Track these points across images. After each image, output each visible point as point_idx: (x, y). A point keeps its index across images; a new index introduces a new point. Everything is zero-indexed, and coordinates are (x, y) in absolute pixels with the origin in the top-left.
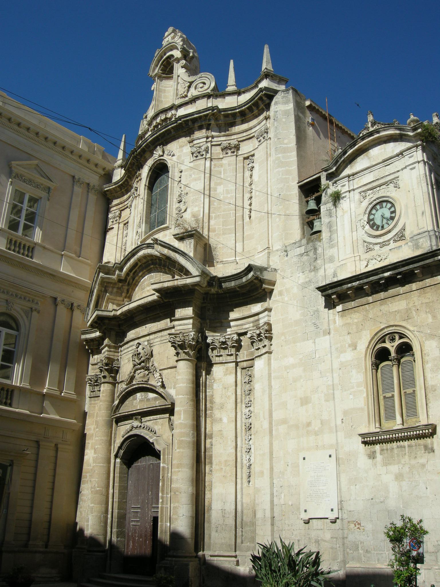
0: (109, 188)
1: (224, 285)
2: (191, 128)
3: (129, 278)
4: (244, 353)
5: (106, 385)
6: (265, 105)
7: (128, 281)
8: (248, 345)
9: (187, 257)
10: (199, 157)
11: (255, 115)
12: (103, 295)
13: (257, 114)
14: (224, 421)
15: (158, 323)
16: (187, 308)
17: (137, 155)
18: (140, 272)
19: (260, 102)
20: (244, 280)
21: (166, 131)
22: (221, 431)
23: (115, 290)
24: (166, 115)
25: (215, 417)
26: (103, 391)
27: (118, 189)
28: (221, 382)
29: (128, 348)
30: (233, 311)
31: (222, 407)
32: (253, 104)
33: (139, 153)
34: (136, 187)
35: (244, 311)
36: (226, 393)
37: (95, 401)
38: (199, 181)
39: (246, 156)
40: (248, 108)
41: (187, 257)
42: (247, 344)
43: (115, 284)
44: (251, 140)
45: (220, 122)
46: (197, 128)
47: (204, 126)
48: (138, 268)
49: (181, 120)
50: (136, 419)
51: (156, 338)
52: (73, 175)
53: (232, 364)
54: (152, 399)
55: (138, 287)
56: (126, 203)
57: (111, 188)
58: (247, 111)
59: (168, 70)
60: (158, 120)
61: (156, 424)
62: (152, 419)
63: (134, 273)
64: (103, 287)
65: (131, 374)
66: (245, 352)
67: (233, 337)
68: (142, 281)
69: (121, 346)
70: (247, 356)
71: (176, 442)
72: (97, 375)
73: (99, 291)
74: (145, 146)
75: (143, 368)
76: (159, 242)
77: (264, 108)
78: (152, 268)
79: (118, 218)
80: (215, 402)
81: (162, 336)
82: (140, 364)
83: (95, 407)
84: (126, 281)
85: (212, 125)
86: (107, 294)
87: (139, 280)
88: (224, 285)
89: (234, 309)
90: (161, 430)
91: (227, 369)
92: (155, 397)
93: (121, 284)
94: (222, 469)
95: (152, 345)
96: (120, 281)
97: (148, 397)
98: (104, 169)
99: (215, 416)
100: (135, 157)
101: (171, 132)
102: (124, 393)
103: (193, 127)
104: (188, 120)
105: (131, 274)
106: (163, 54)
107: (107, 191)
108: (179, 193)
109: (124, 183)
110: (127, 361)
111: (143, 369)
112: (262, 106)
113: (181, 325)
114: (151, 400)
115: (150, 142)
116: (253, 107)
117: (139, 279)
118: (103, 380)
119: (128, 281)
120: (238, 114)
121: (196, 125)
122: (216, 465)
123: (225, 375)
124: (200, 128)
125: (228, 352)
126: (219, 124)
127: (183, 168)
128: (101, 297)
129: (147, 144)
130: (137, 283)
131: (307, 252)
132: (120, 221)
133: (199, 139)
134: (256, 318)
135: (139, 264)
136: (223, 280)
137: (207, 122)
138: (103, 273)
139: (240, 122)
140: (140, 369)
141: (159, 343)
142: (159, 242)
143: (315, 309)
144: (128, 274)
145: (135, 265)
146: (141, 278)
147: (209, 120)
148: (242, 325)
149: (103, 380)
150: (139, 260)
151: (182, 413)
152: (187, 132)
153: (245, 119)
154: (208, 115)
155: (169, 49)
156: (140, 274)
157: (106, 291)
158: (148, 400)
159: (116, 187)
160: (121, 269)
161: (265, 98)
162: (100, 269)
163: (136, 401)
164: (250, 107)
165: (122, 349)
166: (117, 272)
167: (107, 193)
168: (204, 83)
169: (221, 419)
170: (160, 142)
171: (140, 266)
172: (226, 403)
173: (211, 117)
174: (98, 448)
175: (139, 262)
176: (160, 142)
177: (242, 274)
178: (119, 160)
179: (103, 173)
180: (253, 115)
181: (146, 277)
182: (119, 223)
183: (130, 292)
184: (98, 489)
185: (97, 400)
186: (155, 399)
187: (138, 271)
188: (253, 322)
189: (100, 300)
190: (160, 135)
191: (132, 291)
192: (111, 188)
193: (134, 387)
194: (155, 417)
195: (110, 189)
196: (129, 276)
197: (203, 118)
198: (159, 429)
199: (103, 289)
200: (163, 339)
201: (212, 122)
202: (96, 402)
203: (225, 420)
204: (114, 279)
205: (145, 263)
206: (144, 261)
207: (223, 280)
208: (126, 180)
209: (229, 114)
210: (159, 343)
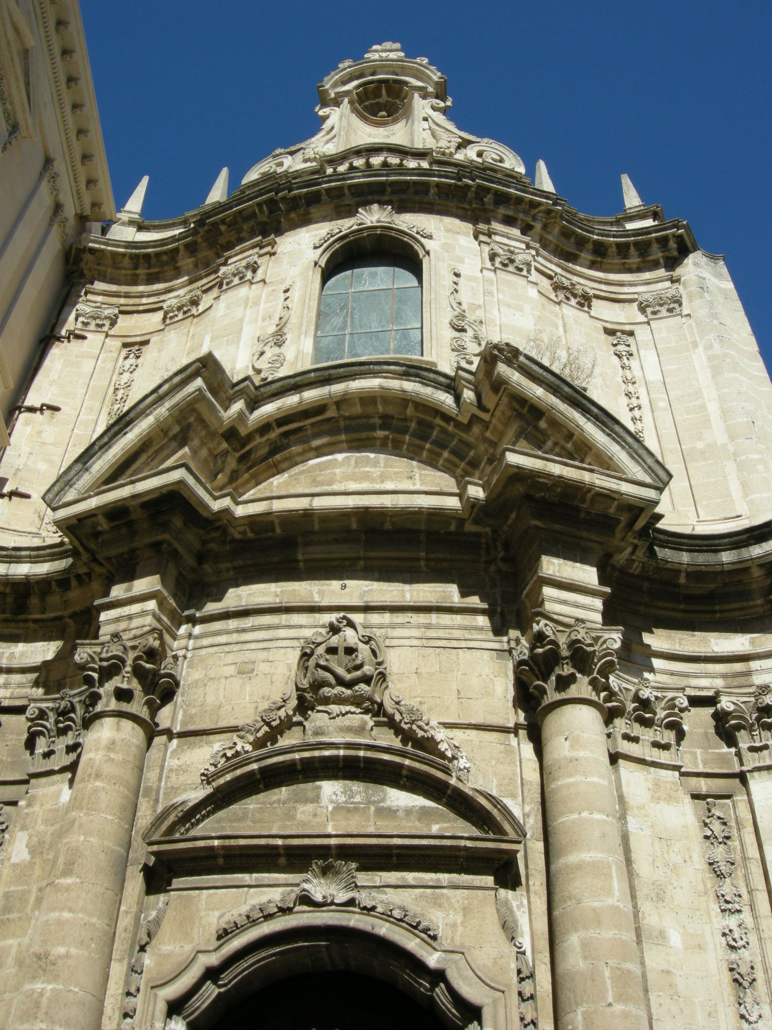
0: (103, 247)
1: (662, 553)
2: (485, 210)
3: (258, 440)
4: (695, 753)
5: (127, 725)
6: (667, 259)
7: (247, 448)
8: (706, 734)
9: (617, 428)
10: (511, 268)
11: (627, 266)
12: (161, 449)
13: (634, 266)
14: (672, 944)
15: (407, 587)
16: (578, 565)
17: (284, 199)
19: (655, 247)
20: (727, 557)
21: (415, 183)
23: (204, 453)
24: (402, 160)
25: (645, 922)
26: (113, 742)
27: (127, 262)
28: (647, 816)
29: (244, 630)
30: (652, 632)
31: (659, 897)
32: (636, 244)
33: (295, 198)
34: (255, 263)
35: (684, 642)
36: (666, 855)
38: (521, 313)
39: (609, 326)
40: (618, 245)
41: (617, 428)
42: (700, 730)
43: (212, 435)
44: (617, 305)
45: (550, 237)
46: (500, 216)
47: (519, 222)
48: (313, 424)
49: (473, 180)
50: (325, 872)
51: (402, 626)
52: (52, 154)
53: (670, 772)
55: (286, 475)
56: (162, 298)
57: (109, 248)
58: (614, 249)
59: (367, 103)
60: (376, 161)
61: (437, 903)
62: (413, 883)
63: (286, 435)
64: (178, 422)
65: (282, 713)
67: (673, 699)
68: (312, 462)
69: (193, 620)
71: (607, 973)
73: (161, 429)
74: (328, 190)
75: (357, 701)
76: (522, 358)
77: (662, 261)
78: (375, 439)
79: (107, 323)
80: (638, 875)
81: (428, 627)
82: (349, 685)
84: (243, 447)
85: (534, 230)
86: (186, 449)
87: (298, 459)
88: (662, 553)
89: (654, 630)
90: (460, 929)
93: (225, 445)
96: (231, 434)
97: (383, 800)
98: (95, 205)
99: (644, 918)
100: (271, 203)
101: (427, 192)
102: (255, 766)
103: (492, 211)
104: (488, 190)
105: (274, 435)
106: (368, 72)
107: (92, 251)
108: (456, 313)
109: (158, 255)
110: (232, 670)
111: (358, 705)
112: (656, 253)
113: (564, 602)
114: (401, 814)
115: (350, 187)
116: (632, 249)
117: (304, 452)
118: (113, 705)
119: (247, 448)
120: (590, 246)
121: (502, 211)
123: (656, 799)
124: (509, 221)
126: (546, 239)
127: (460, 269)
128: (151, 451)
129: (340, 188)
130: (284, 465)
132: (111, 332)
133: (509, 238)
134: (738, 667)
135: (331, 413)
136: (661, 536)
137: (529, 220)
138: (205, 381)
139: (588, 263)
142: (522, 358)
144: (265, 428)
145: (319, 409)
146: (312, 454)
147: (534, 218)
149: (113, 705)
150: (342, 401)
151: (614, 874)
152: (469, 213)
153: (601, 262)
154: (540, 204)
155: (387, 69)
156: (316, 443)
157: (182, 440)
158: (390, 813)
159: (124, 255)
160: (253, 405)
161: (672, 245)
162: (204, 366)
163: (310, 807)
164: (627, 245)
165: (198, 630)
166: (238, 406)
167: (87, 257)
169: (662, 935)
170: (386, 198)
171: (329, 420)
172: (672, 888)
173: (541, 214)
174: (67, 955)
175: (334, 407)
176: (386, 198)
177: (726, 540)
178: (125, 211)
179: (79, 212)
180: (624, 264)
181: (340, 457)
182: (107, 336)
183: (240, 481)
186: (423, 813)
187: (309, 432)
189: (143, 458)
190: (393, 183)
191: (248, 481)
192: (109, 248)
193: (327, 753)
194: (429, 877)
195: (102, 251)
196: (262, 435)
197: (523, 206)
198: (454, 926)
199: (176, 429)
200: (432, 633)
201: (538, 226)
203: (675, 939)
204: (220, 419)
205: (350, 418)
206: (358, 410)
207: (661, 536)
208: (176, 251)
209: (574, 233)
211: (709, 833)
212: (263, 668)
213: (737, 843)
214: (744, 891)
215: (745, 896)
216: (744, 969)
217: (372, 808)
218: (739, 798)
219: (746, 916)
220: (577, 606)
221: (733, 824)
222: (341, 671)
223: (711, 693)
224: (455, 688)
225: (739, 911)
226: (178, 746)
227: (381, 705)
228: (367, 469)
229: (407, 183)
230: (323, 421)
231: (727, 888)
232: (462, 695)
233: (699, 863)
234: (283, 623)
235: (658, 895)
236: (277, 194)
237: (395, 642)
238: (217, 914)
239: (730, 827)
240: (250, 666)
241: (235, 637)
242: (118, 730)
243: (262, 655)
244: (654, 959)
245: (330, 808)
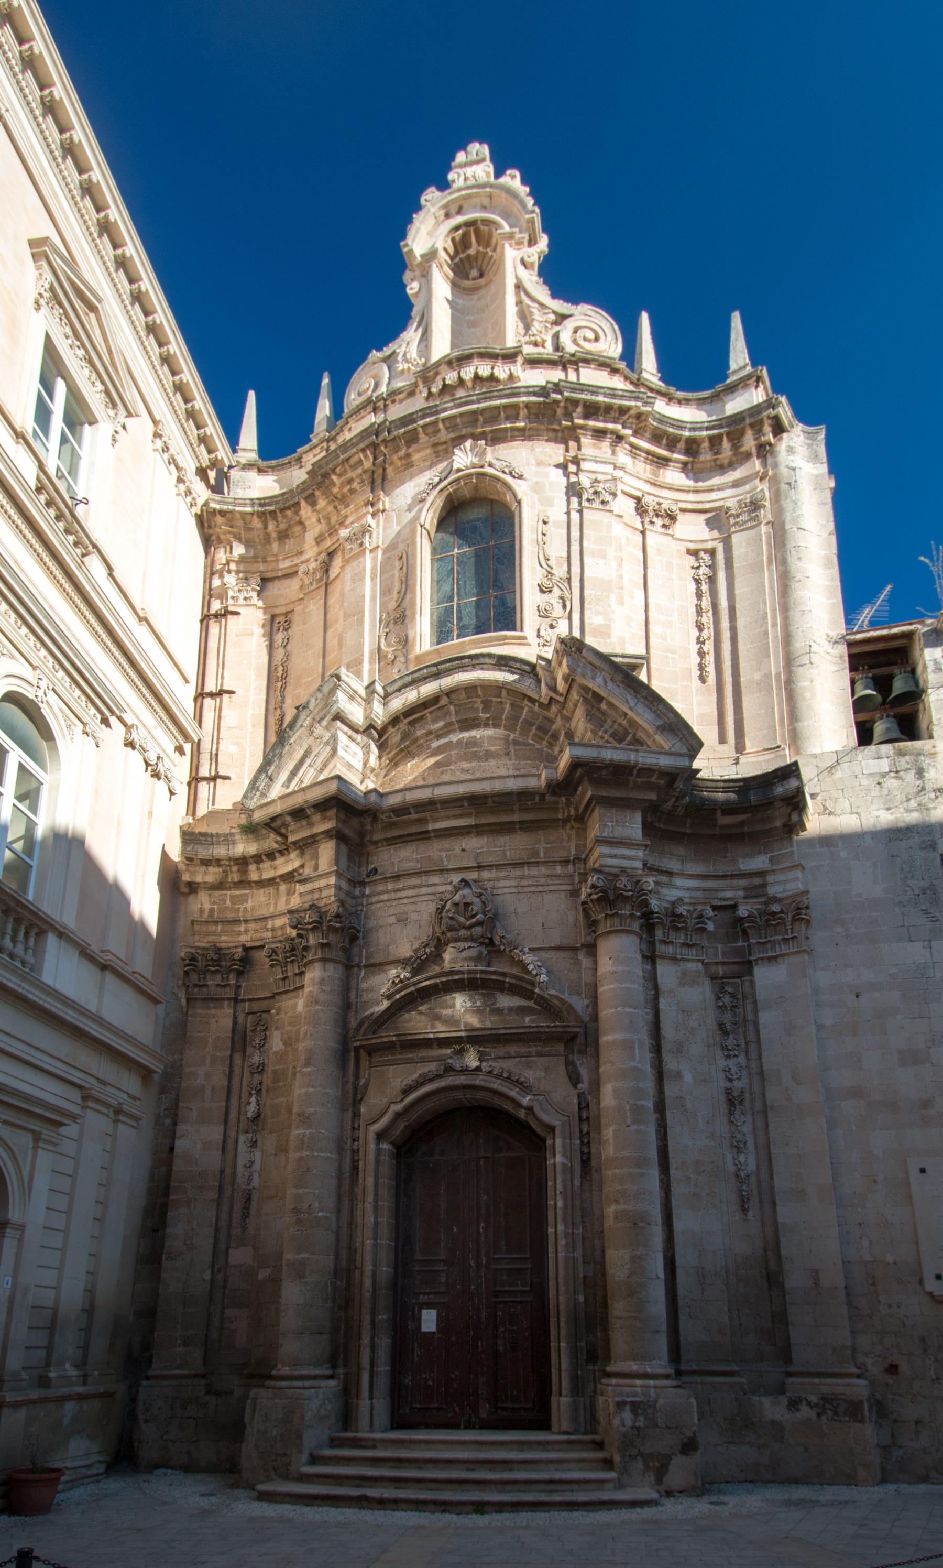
4: (717, 948)
14: (685, 1079)
18: (435, 721)
22: (681, 1098)
29: (399, 890)
31: (679, 1049)
37: (209, 1008)
51: (505, 878)
54: (510, 1010)
61: (529, 1066)
63: (411, 723)
66: (720, 946)
70: (724, 954)
72: (220, 949)
83: (208, 1023)
91: (684, 973)
92: (519, 1007)
94: (689, 1178)
95: (495, 892)
97: (494, 1004)
110: (392, 920)
114: (506, 1012)
122: (677, 1168)
123: (682, 984)
125: (683, 938)
131: (897, 772)
140: (466, 939)
141: (513, 890)
143: (922, 884)
148: (716, 890)
168: (597, 339)
169: (679, 1075)
184: (320, 1214)
185: (215, 1008)
186: (521, 1010)
188: (745, 889)
198: (539, 1079)
200: (525, 882)
202: (213, 1011)
203: (688, 1077)
210: (513, 890)
211: (721, 1004)
212: (414, 916)
213: (741, 1010)
214: (742, 1042)
215: (743, 1045)
216: (735, 1093)
217: (488, 1009)
218: (746, 978)
219: (742, 1059)
220: (624, 857)
221: (740, 997)
222: (462, 920)
223: (732, 903)
224: (540, 921)
225: (736, 1056)
226: (365, 974)
227: (491, 940)
228: (475, 749)
229: (497, 408)
230: (439, 708)
231: (730, 1042)
232: (546, 926)
233: (711, 1023)
234: (424, 883)
235: (678, 1049)
236: (377, 436)
237: (500, 891)
238: (399, 1080)
239: (737, 999)
240: (405, 916)
241: (393, 895)
242: (325, 970)
243: (412, 907)
244: (671, 1091)
245: (462, 1010)
